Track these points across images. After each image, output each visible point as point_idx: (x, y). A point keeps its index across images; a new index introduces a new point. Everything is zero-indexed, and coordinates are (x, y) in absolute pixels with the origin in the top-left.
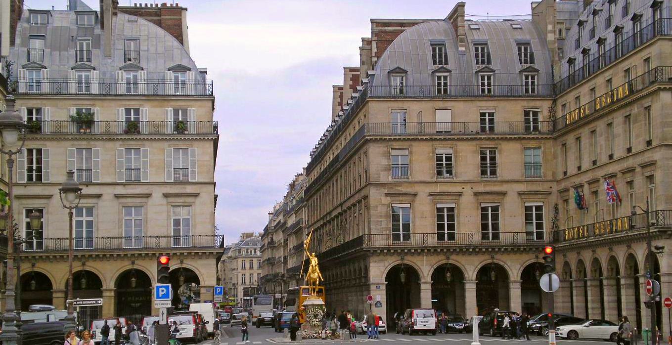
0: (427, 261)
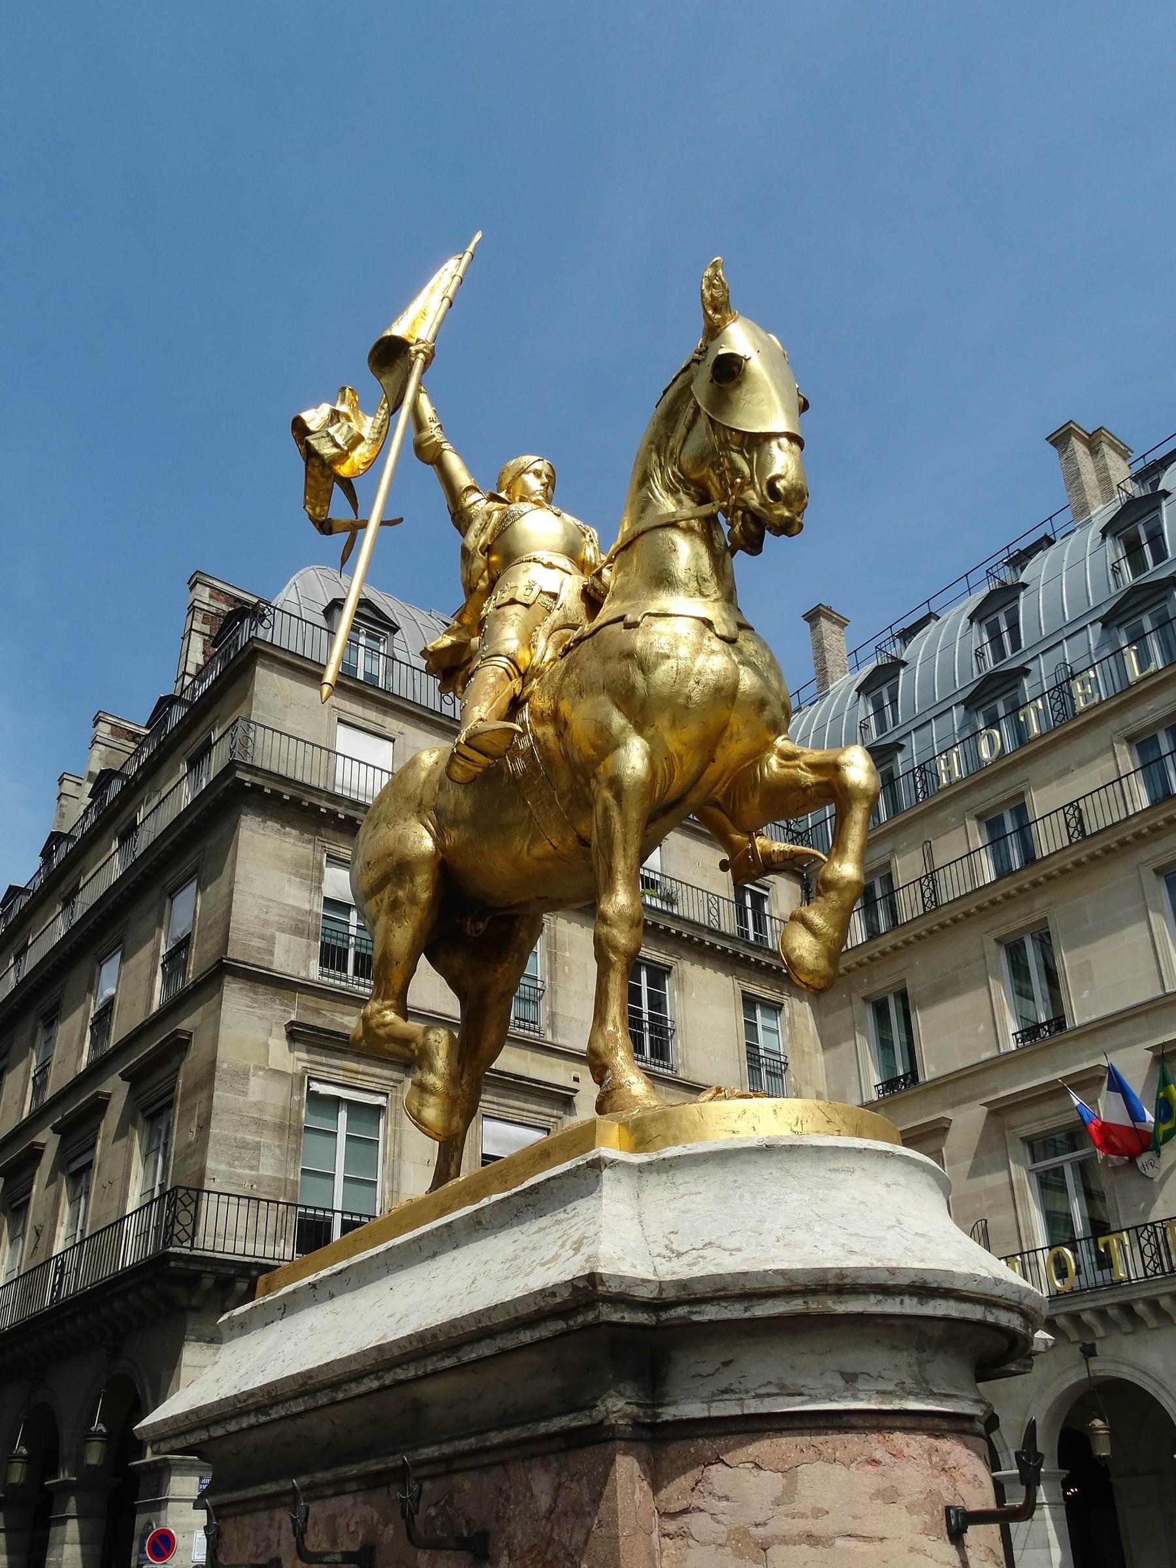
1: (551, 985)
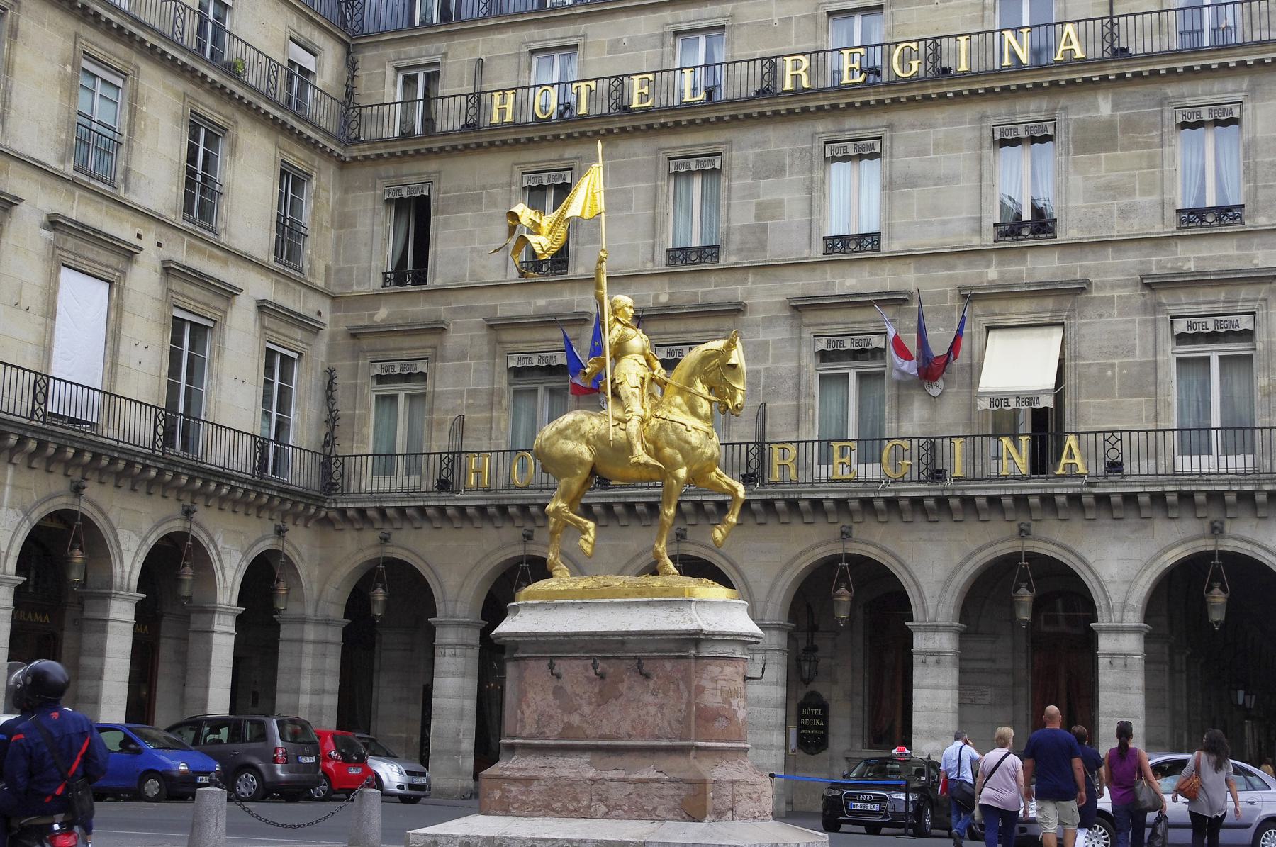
0: (14, 486)
1: (128, 140)
